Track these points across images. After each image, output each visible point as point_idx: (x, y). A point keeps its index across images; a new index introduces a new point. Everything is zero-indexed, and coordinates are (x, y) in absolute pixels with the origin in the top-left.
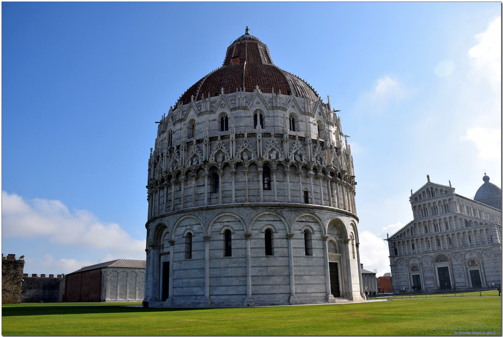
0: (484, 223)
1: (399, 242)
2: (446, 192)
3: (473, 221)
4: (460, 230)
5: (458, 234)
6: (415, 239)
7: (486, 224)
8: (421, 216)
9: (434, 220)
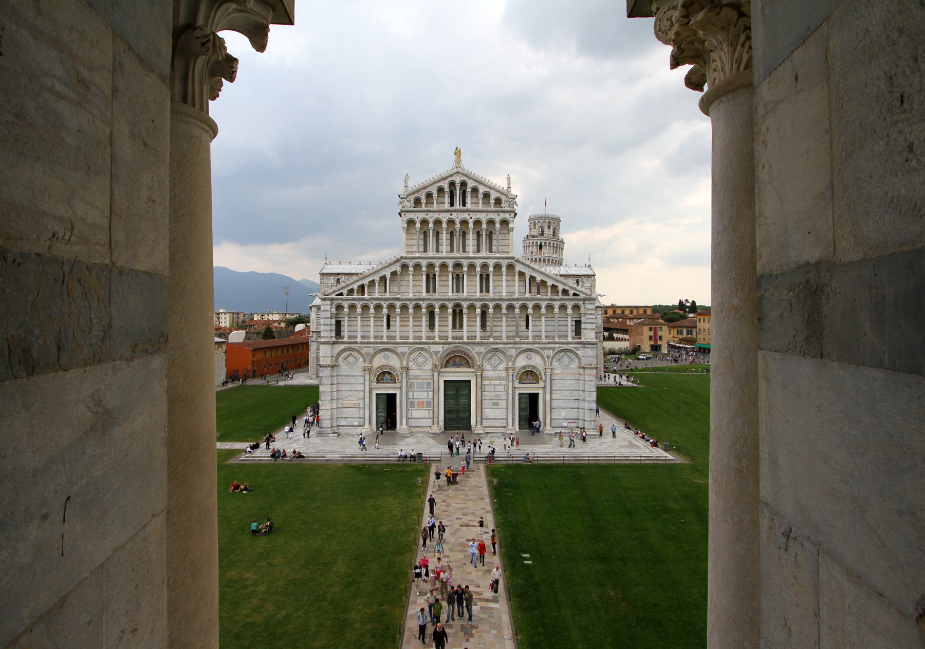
0: (571, 292)
1: (352, 307)
2: (498, 201)
3: (550, 283)
4: (517, 299)
5: (511, 307)
6: (398, 304)
7: (575, 295)
8: (422, 249)
9: (458, 266)
